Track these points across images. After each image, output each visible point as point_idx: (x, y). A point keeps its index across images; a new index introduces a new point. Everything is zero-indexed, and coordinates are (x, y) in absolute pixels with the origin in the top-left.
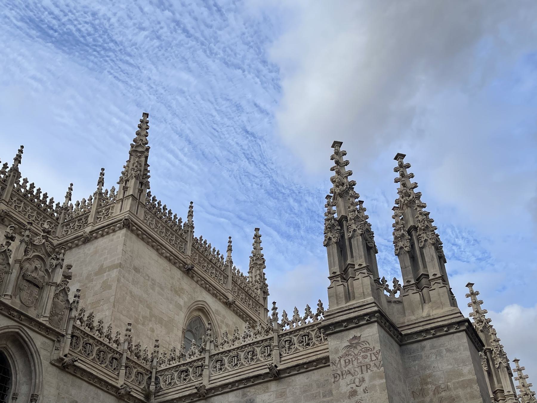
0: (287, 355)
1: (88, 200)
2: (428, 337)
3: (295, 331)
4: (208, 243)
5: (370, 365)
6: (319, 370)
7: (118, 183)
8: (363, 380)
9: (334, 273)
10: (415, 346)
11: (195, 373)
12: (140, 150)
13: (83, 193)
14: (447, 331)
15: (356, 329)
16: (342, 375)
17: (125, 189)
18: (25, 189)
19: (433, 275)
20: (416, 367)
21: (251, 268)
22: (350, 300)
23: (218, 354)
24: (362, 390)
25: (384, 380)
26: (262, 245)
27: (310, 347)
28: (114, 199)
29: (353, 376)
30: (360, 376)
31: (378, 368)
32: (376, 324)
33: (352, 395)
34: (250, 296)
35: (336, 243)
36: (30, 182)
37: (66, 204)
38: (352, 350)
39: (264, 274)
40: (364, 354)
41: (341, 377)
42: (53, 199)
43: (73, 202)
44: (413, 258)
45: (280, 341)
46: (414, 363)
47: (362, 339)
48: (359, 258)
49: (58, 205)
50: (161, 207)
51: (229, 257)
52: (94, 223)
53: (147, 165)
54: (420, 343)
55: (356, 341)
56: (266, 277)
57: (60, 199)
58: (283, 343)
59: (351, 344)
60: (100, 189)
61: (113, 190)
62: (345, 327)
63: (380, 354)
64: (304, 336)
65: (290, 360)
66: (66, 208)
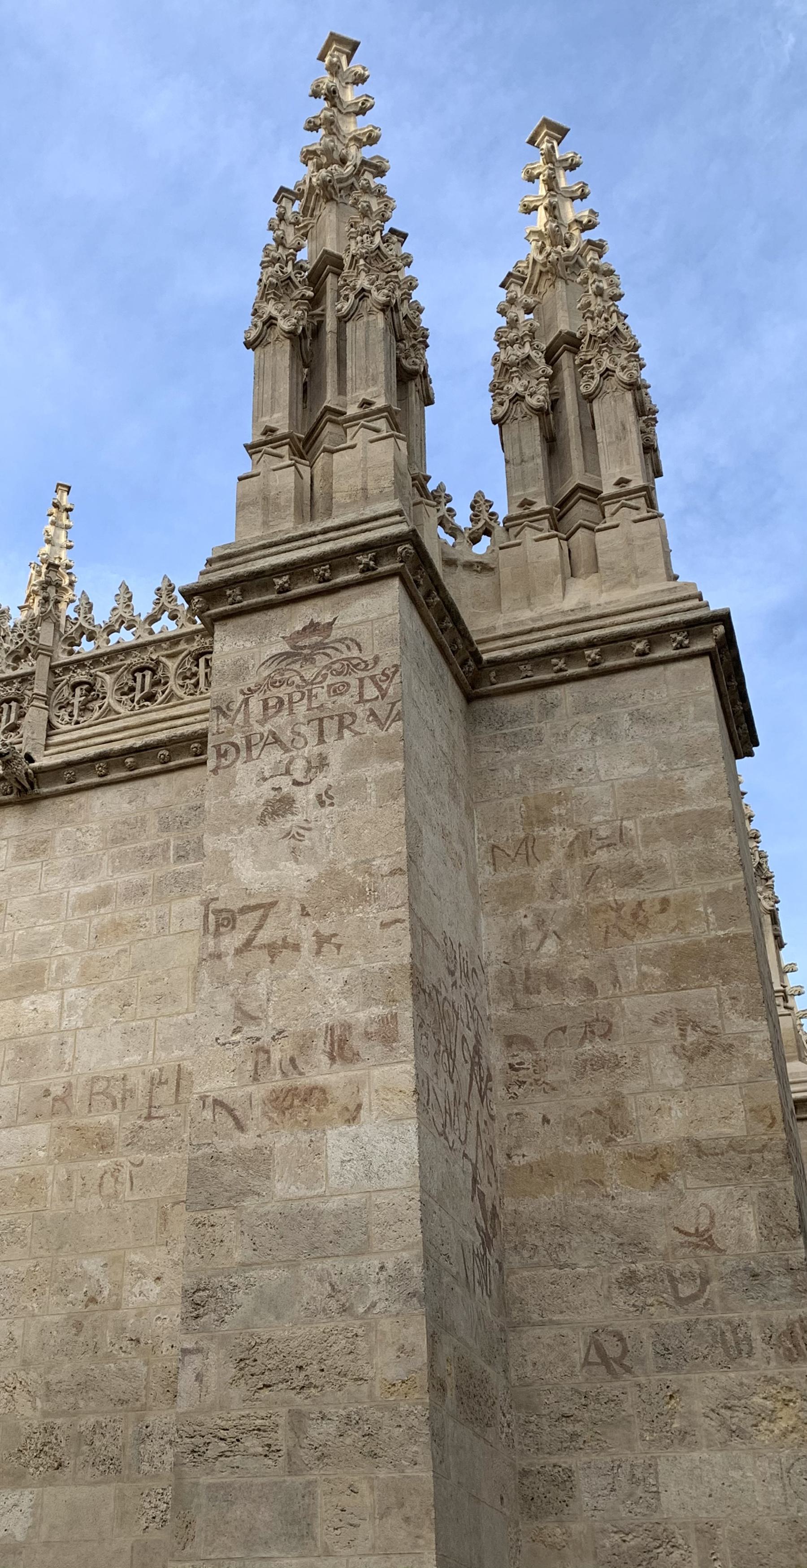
0: (74, 727)
2: (570, 671)
3: (112, 655)
5: (353, 715)
6: (175, 775)
8: (322, 763)
10: (520, 701)
14: (642, 654)
15: (319, 602)
16: (249, 748)
19: (618, 483)
20: (517, 768)
22: (312, 519)
24: (312, 796)
25: (400, 765)
29: (287, 750)
30: (312, 749)
31: (381, 725)
32: (396, 583)
33: (275, 814)
35: (291, 334)
38: (297, 666)
40: (339, 679)
41: (243, 754)
44: (552, 443)
45: (56, 684)
46: (512, 757)
47: (336, 634)
48: (366, 380)
54: (540, 693)
55: (316, 639)
58: (66, 692)
59: (294, 647)
62: (283, 590)
63: (397, 679)
64: (142, 669)
65: (81, 744)
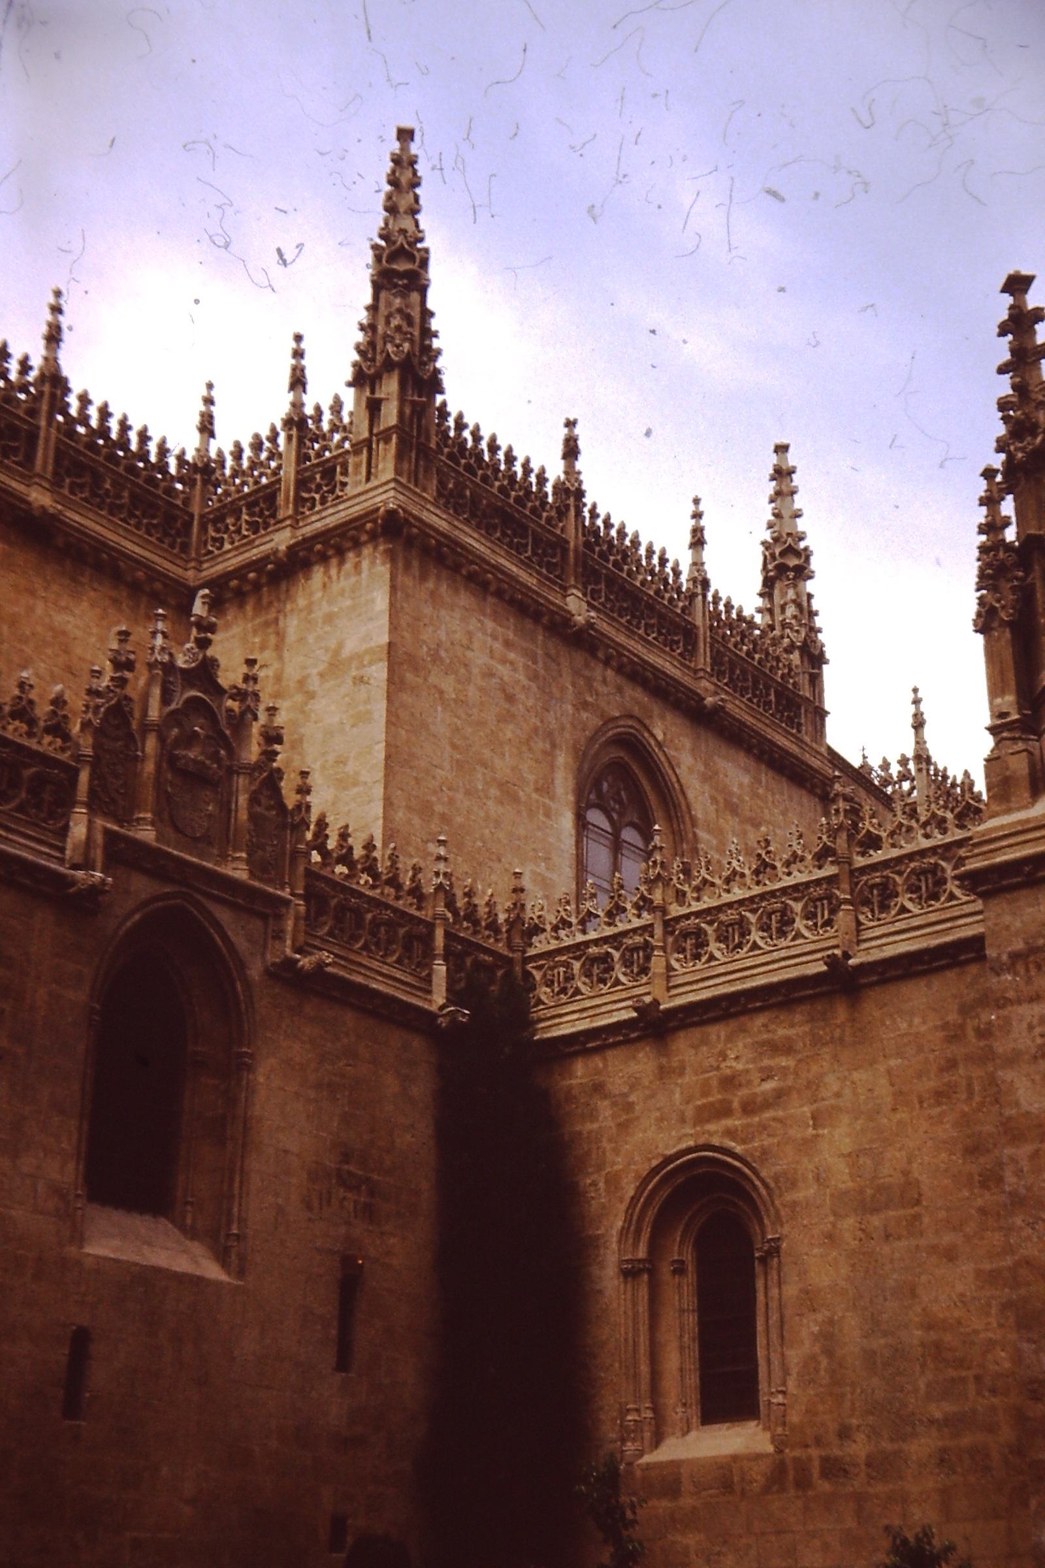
1: (268, 439)
4: (629, 531)
7: (349, 384)
9: (1002, 715)
11: (627, 963)
12: (400, 270)
13: (251, 415)
17: (374, 407)
18: (86, 424)
21: (769, 584)
23: (687, 917)
26: (799, 502)
27: (938, 905)
28: (344, 439)
34: (764, 682)
35: (1010, 624)
36: (97, 402)
37: (202, 451)
39: (810, 596)
42: (163, 441)
43: (222, 443)
49: (181, 458)
50: (484, 445)
51: (698, 565)
52: (296, 520)
53: (427, 314)
56: (816, 605)
57: (183, 440)
60: (297, 405)
61: (337, 407)
66: (207, 465)
